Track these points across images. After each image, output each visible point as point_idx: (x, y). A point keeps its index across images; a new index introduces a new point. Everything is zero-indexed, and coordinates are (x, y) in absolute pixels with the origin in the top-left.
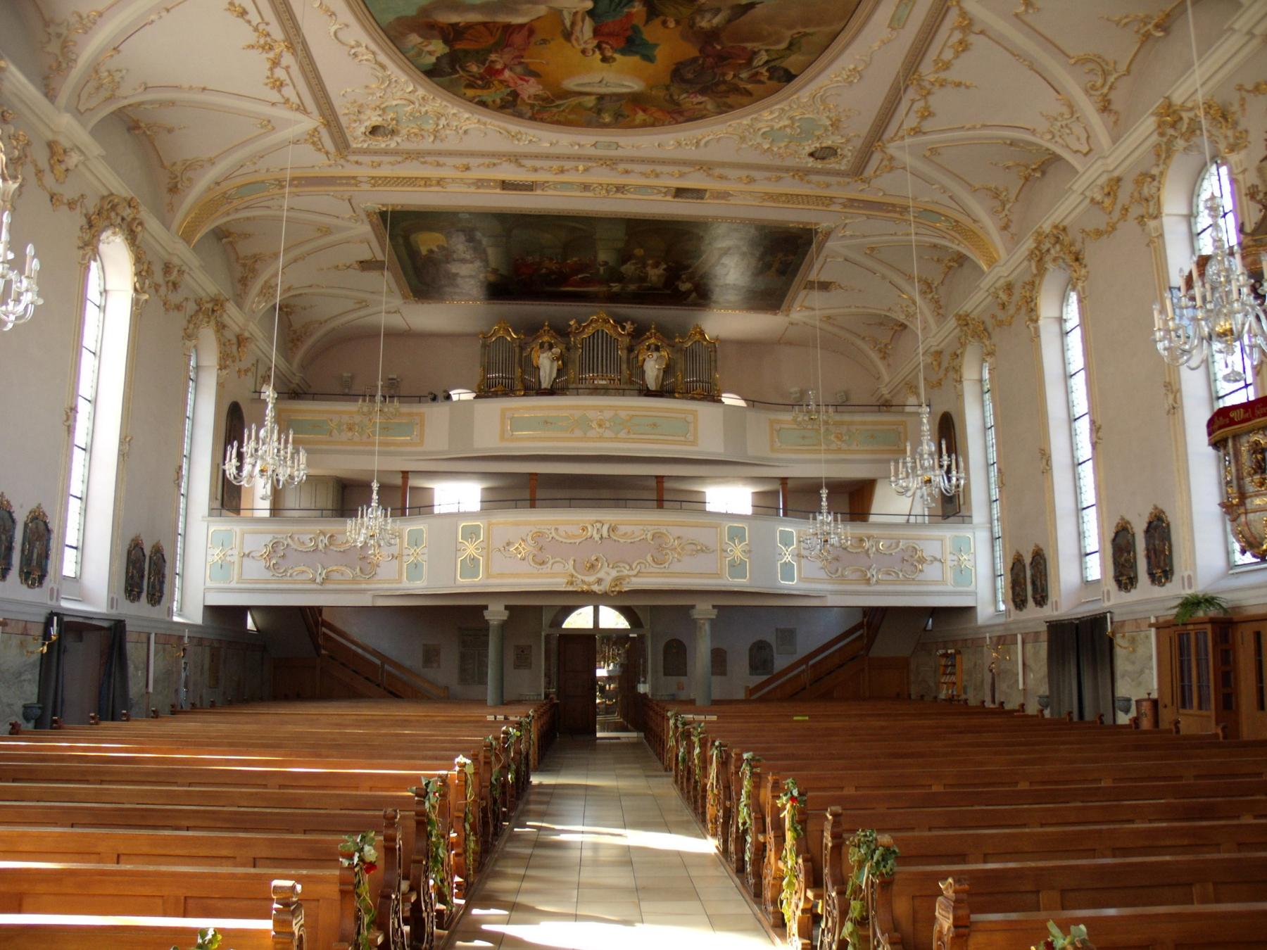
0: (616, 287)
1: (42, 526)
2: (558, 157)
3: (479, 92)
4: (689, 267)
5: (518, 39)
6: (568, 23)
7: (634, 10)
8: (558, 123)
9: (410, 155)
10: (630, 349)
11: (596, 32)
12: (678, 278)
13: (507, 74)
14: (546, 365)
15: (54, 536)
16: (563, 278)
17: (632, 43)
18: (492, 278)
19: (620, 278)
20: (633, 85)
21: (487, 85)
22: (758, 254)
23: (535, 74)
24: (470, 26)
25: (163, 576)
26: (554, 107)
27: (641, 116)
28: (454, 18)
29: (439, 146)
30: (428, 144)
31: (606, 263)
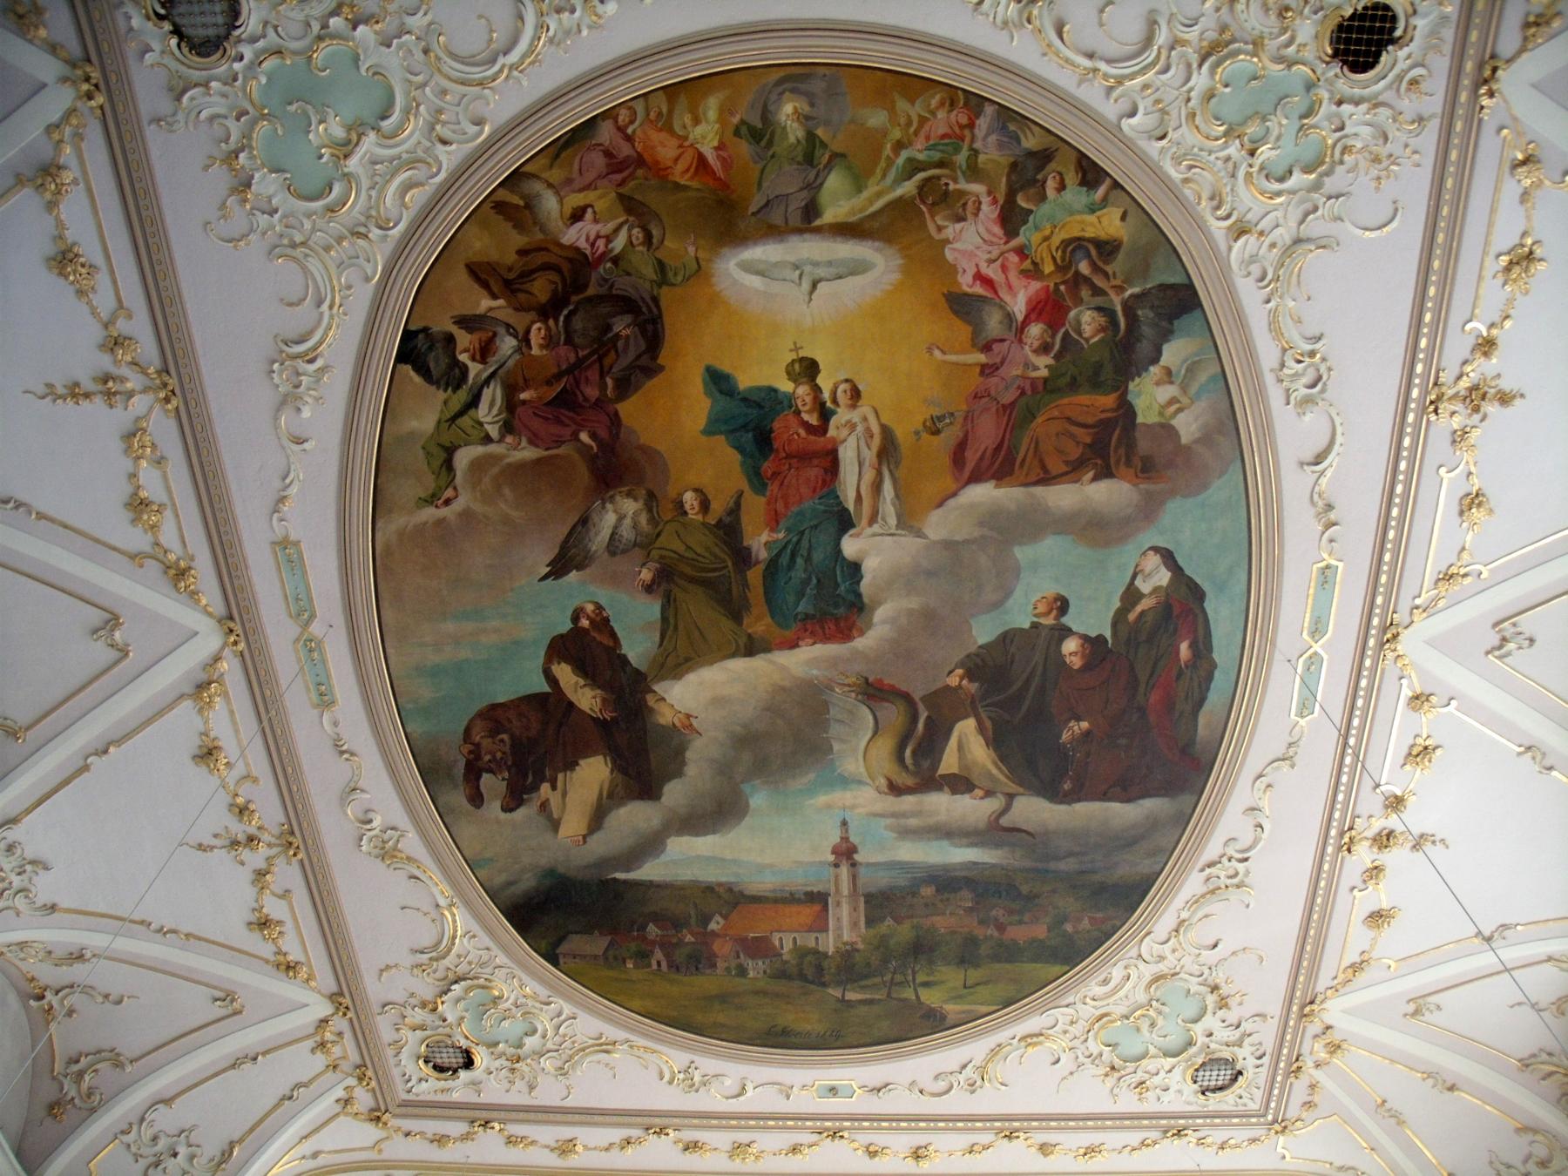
6: (888, 487)
7: (764, 537)
11: (830, 461)
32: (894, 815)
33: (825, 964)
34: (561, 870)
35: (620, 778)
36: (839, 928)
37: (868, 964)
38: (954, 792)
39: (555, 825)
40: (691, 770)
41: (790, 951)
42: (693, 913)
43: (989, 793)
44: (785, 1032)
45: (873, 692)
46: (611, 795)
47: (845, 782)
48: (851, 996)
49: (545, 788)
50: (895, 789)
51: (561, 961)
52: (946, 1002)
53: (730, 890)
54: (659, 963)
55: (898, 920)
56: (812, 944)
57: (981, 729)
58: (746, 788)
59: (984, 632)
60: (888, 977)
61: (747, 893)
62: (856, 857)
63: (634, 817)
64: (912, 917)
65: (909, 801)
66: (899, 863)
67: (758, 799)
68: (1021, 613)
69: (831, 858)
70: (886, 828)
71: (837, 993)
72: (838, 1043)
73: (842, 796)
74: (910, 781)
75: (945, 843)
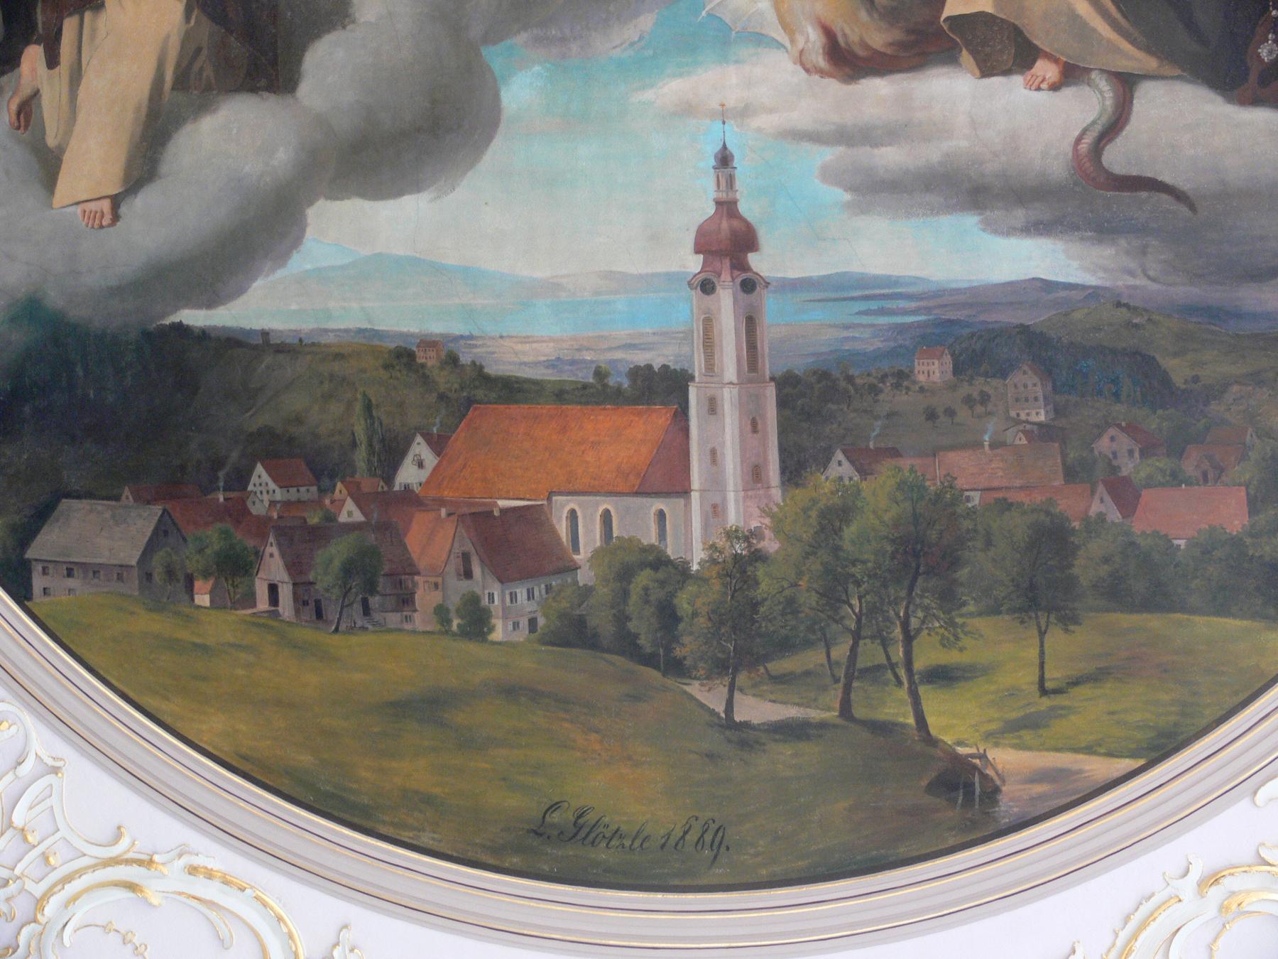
32: (843, 136)
33: (683, 603)
34: (54, 299)
35: (207, 29)
36: (716, 482)
37: (791, 606)
38: (987, 70)
39: (48, 166)
41: (597, 554)
42: (360, 430)
43: (1071, 74)
44: (581, 830)
46: (182, 81)
48: (755, 709)
49: (33, 55)
50: (846, 61)
51: (38, 582)
52: (992, 737)
53: (453, 360)
54: (273, 589)
55: (864, 461)
58: (494, 56)
60: (841, 651)
61: (492, 370)
62: (753, 259)
63: (236, 140)
64: (895, 453)
65: (878, 94)
66: (863, 282)
67: (522, 88)
69: (694, 264)
70: (830, 175)
71: (712, 697)
72: (719, 873)
73: (717, 81)
74: (879, 38)
75: (971, 221)
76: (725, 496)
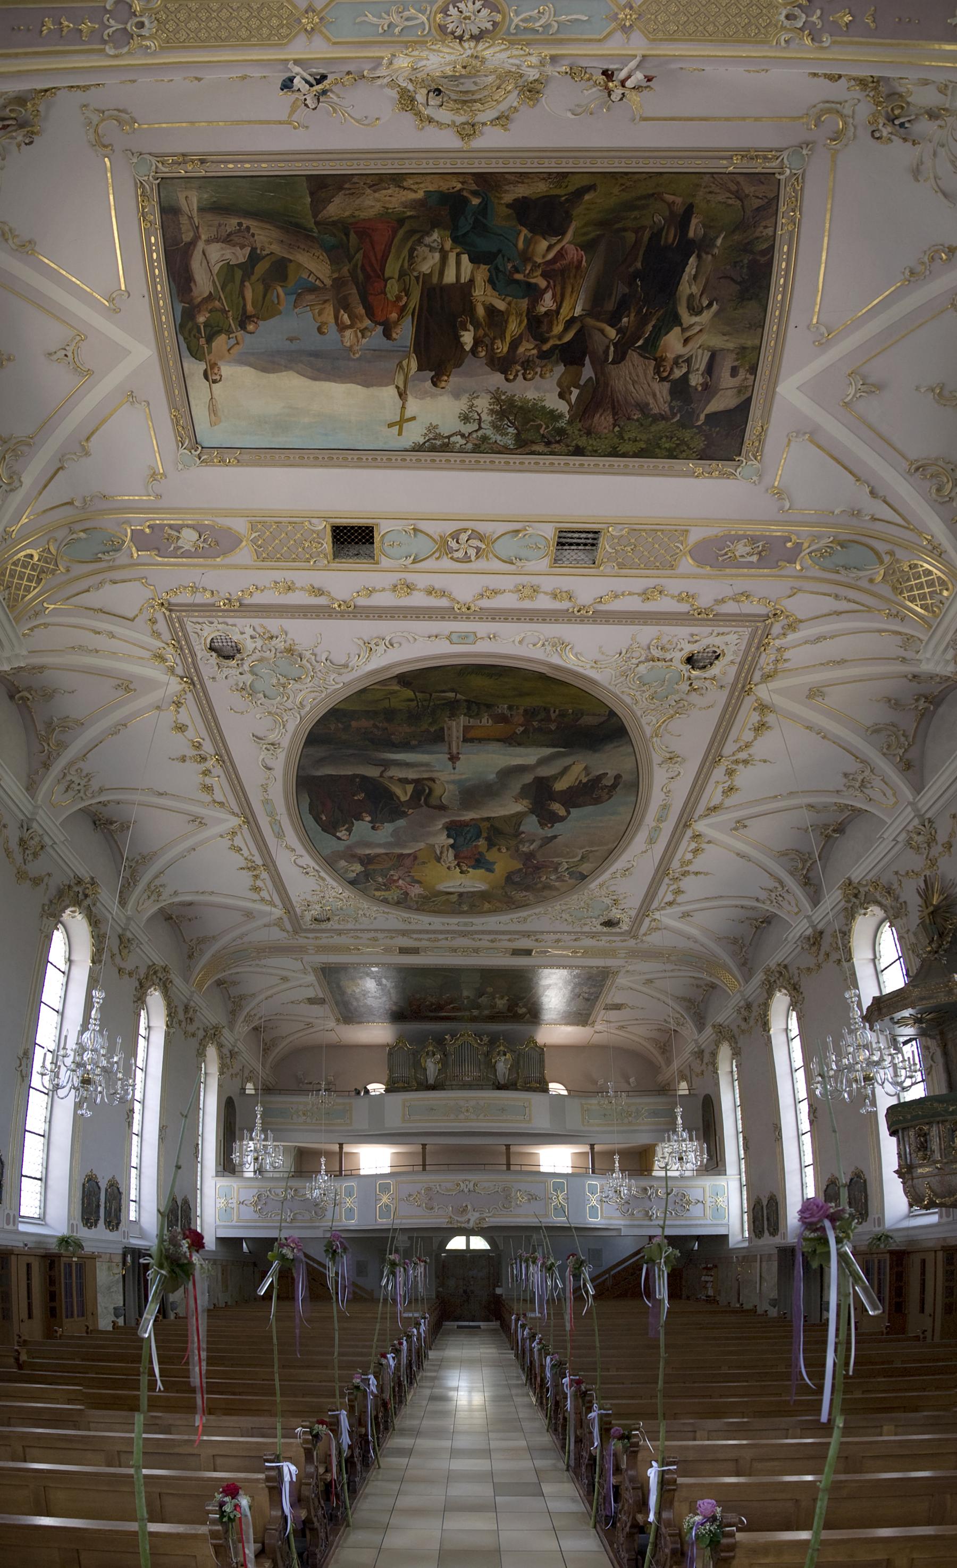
0: (475, 1012)
1: (116, 1191)
2: (434, 932)
3: (383, 893)
4: (524, 998)
5: (407, 862)
6: (438, 853)
8: (434, 912)
9: (340, 932)
10: (487, 1054)
11: (456, 857)
12: (517, 1005)
13: (401, 882)
14: (432, 1067)
15: (123, 1196)
16: (440, 1008)
17: (479, 862)
18: (394, 1008)
19: (478, 1007)
20: (481, 886)
21: (388, 889)
22: (570, 988)
23: (419, 882)
24: (379, 855)
25: (190, 1219)
26: (433, 902)
27: (487, 906)
28: (368, 852)
29: (358, 927)
30: (350, 926)
31: (469, 997)
32: (432, 771)
33: (465, 711)
38: (406, 778)
40: (519, 786)
44: (490, 676)
45: (442, 808)
47: (453, 782)
50: (433, 780)
56: (471, 720)
57: (398, 798)
59: (401, 822)
60: (432, 704)
65: (426, 776)
68: (388, 828)
71: (459, 696)
74: (426, 782)
76: (456, 727)
